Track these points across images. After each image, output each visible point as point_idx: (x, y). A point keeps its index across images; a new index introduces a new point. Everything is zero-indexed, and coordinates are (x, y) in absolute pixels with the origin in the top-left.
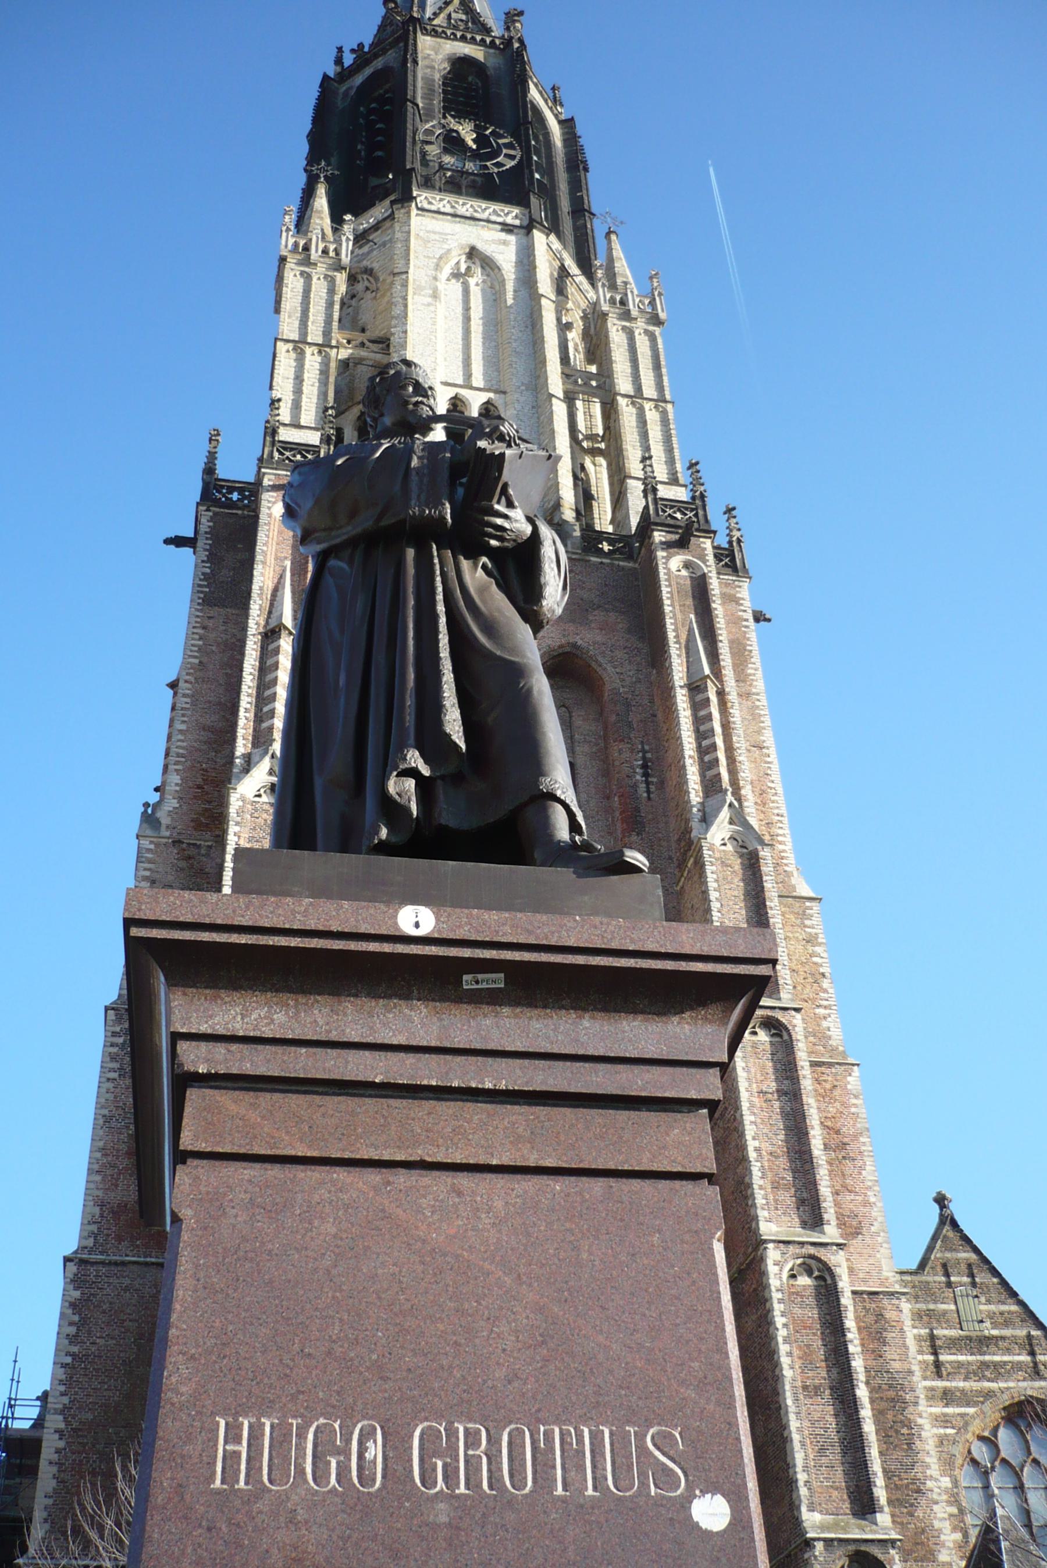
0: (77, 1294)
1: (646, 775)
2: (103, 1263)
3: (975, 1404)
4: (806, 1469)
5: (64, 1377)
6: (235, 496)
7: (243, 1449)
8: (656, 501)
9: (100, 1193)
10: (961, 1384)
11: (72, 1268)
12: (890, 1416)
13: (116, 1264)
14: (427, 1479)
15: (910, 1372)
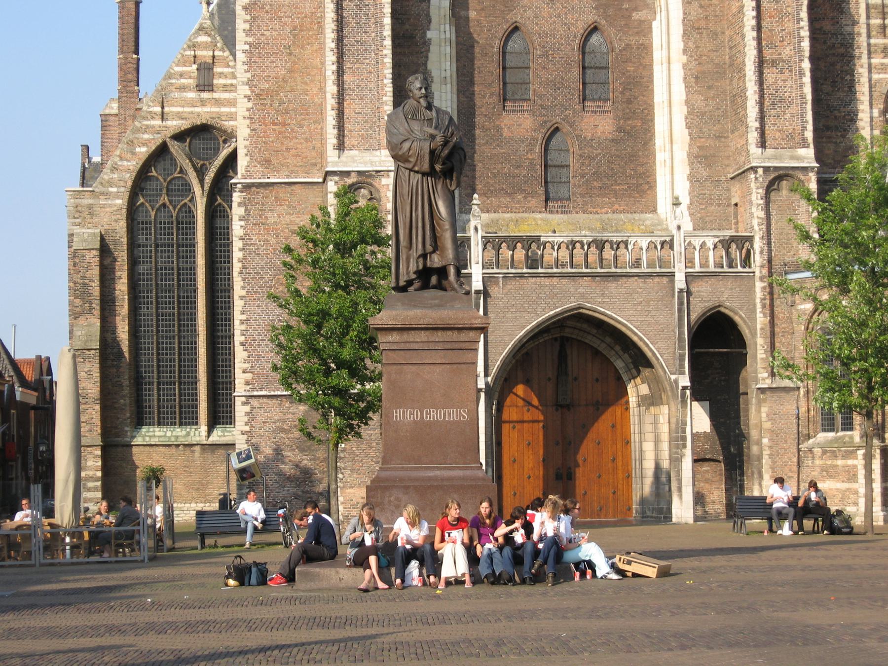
4: (802, 74)
5: (245, 59)
12: (838, 67)
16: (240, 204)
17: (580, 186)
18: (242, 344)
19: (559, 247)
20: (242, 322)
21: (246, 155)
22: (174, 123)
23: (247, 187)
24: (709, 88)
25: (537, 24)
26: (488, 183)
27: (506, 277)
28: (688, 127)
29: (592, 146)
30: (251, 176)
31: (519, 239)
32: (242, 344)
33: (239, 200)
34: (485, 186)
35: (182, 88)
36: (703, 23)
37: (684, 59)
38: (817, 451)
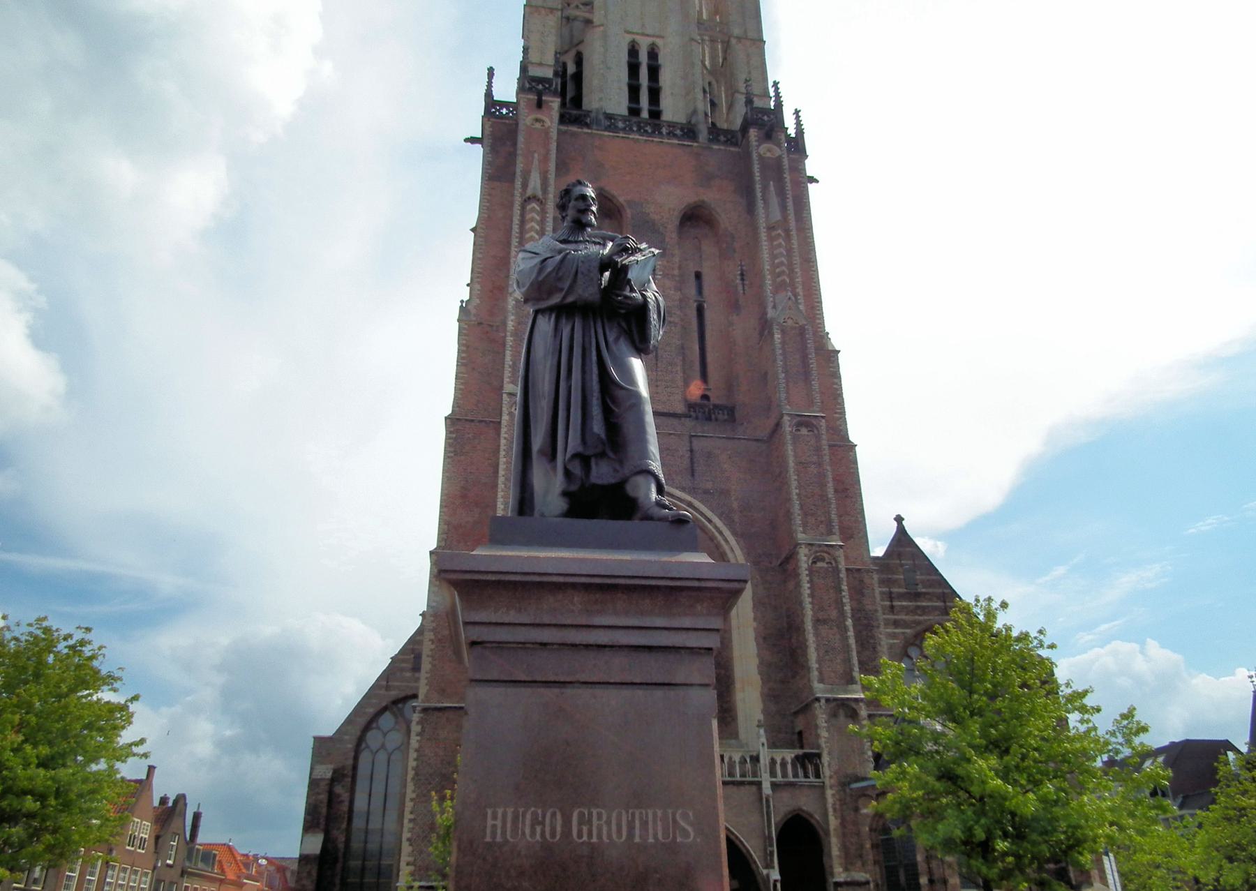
1: (742, 280)
6: (504, 111)
7: (499, 823)
8: (752, 109)
14: (580, 835)
18: (409, 840)
20: (411, 821)
23: (425, 710)
32: (409, 840)
35: (402, 670)
37: (755, 624)
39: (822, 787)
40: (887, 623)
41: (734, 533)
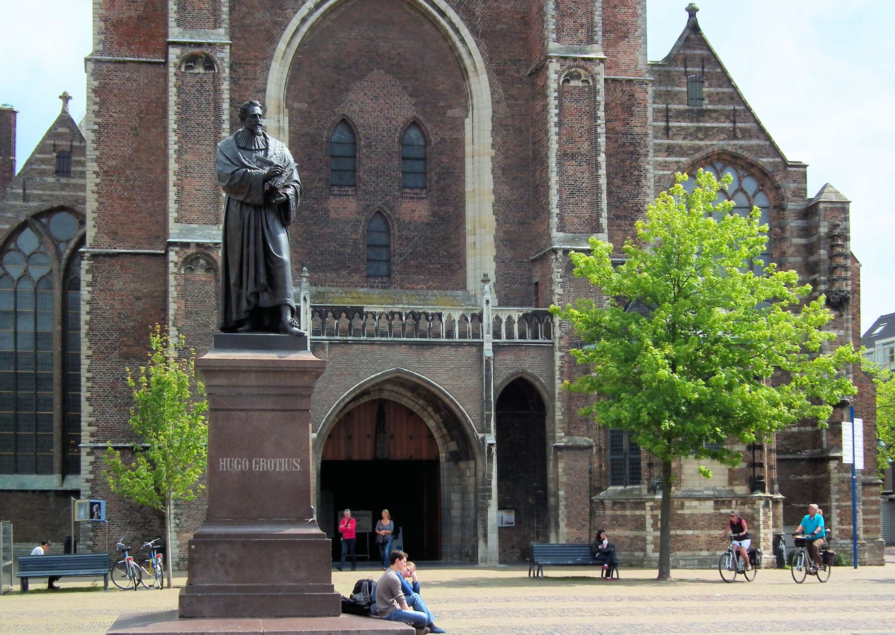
0: (96, 83)
2: (110, 62)
3: (688, 155)
5: (94, 138)
9: (102, 11)
10: (680, 142)
11: (91, 66)
12: (628, 163)
13: (119, 62)
15: (646, 134)
16: (87, 272)
17: (398, 265)
18: (88, 399)
19: (380, 318)
20: (88, 379)
21: (94, 226)
22: (35, 204)
23: (95, 256)
24: (515, 179)
25: (362, 118)
26: (316, 259)
27: (332, 344)
28: (494, 214)
29: (409, 229)
30: (98, 246)
31: (344, 309)
32: (88, 399)
33: (87, 268)
34: (313, 262)
35: (43, 173)
36: (509, 122)
37: (493, 152)
38: (608, 503)
39: (551, 348)
40: (658, 149)
41: (474, 32)
